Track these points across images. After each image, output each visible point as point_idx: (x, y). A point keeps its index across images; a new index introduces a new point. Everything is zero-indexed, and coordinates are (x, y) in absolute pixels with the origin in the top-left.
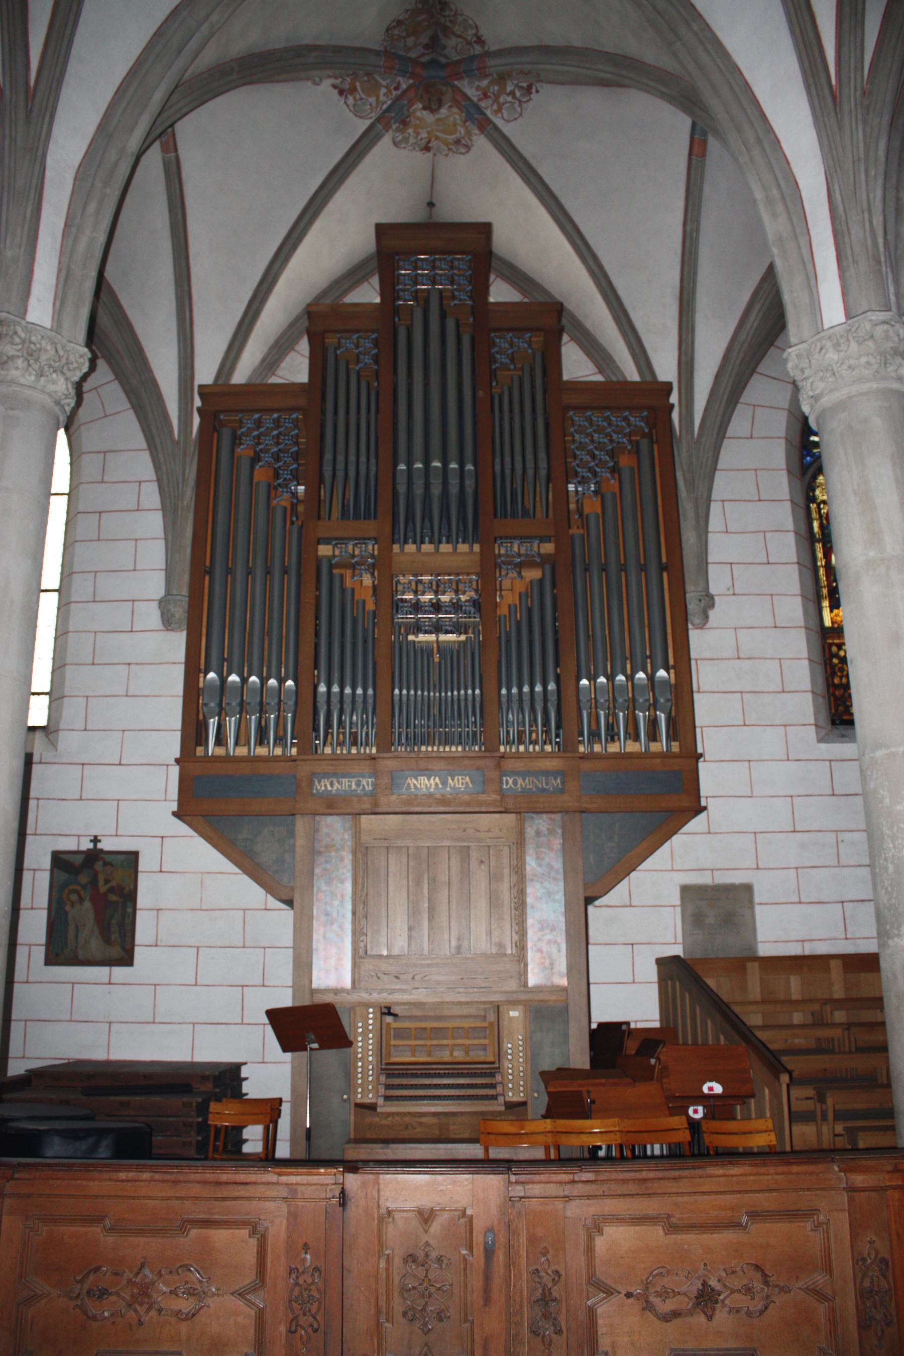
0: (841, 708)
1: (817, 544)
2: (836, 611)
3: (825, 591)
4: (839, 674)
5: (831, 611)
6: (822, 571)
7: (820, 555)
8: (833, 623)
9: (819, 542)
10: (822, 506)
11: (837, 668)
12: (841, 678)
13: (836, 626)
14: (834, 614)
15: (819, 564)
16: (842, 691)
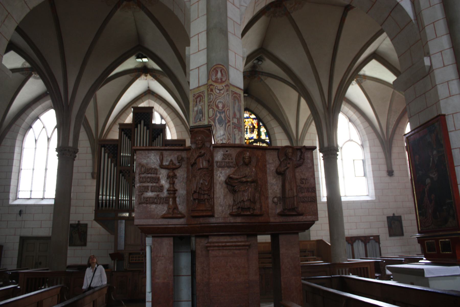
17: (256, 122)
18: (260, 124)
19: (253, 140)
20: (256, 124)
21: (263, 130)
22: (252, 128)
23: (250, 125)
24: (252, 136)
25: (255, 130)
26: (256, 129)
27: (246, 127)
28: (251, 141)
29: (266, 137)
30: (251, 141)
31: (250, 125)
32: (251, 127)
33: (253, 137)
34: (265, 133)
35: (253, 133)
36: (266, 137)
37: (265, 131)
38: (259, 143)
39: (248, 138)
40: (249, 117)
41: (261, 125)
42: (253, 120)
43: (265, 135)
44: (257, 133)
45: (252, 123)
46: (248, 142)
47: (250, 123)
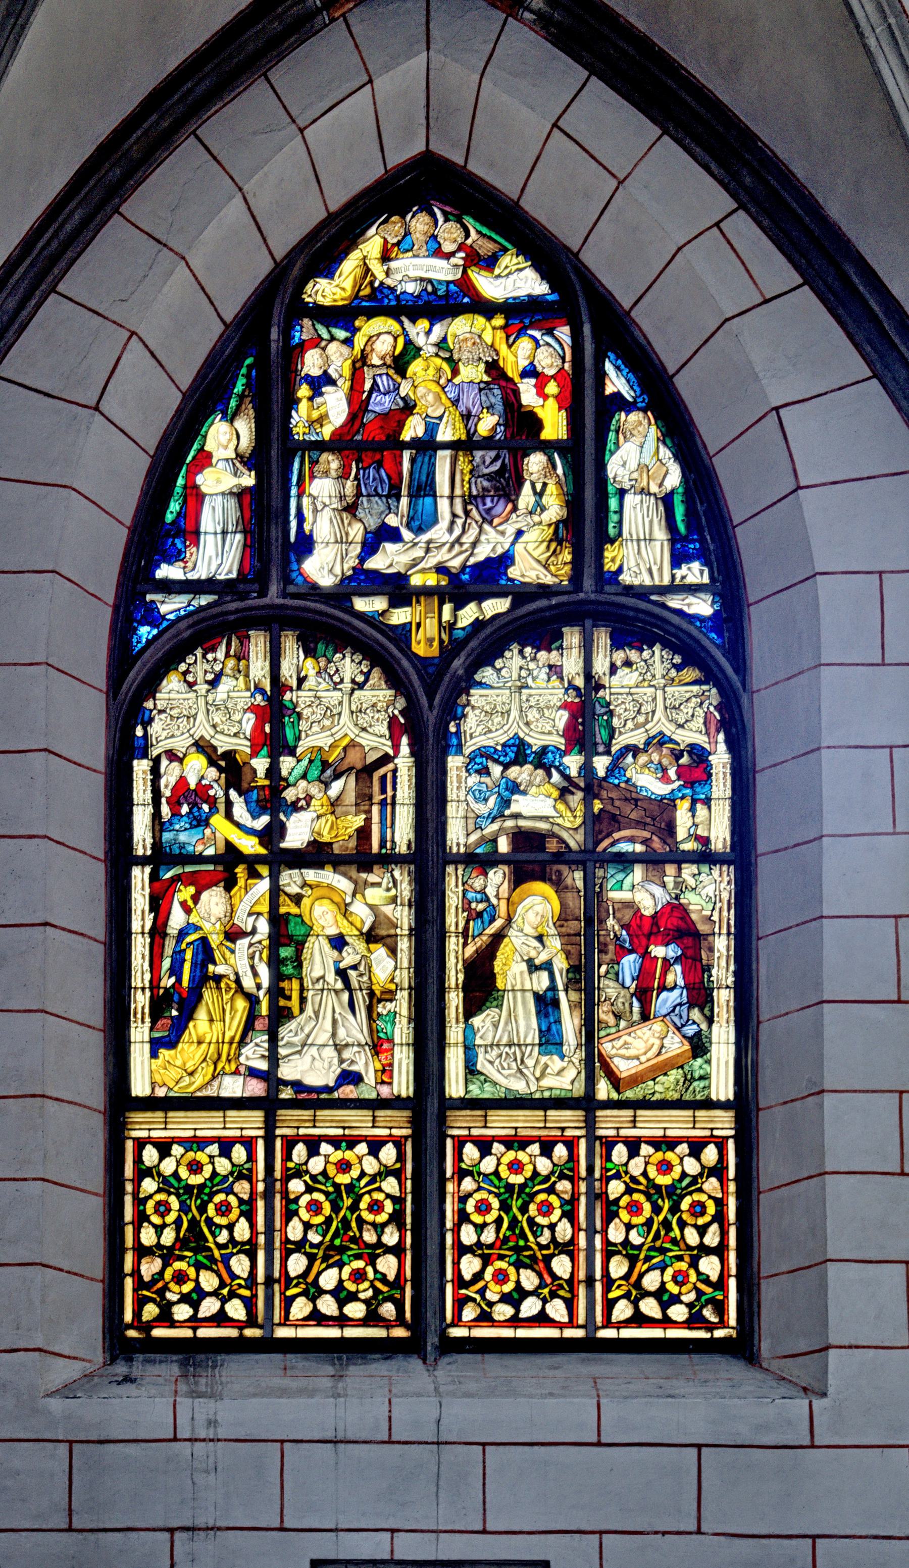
0: (150, 1311)
1: (136, 871)
2: (164, 1053)
3: (141, 1001)
4: (156, 1219)
5: (154, 1055)
6: (140, 947)
7: (140, 900)
8: (153, 1085)
9: (143, 861)
10: (164, 762)
11: (150, 1204)
12: (159, 1229)
13: (161, 1092)
14: (160, 1061)
15: (136, 926)
16: (158, 1263)
17: (547, 362)
18: (601, 377)
19: (496, 606)
20: (552, 388)
21: (643, 468)
22: (488, 443)
23: (470, 399)
24: (482, 553)
25: (535, 462)
26: (547, 447)
27: (413, 429)
28: (469, 614)
29: (677, 560)
30: (469, 614)
31: (470, 399)
32: (486, 424)
33: (506, 559)
34: (667, 500)
35: (503, 508)
36: (677, 560)
37: (674, 478)
38: (572, 637)
39: (432, 580)
40: (465, 284)
41: (618, 403)
42: (513, 332)
43: (661, 534)
44: (554, 509)
45: (494, 368)
46: (431, 628)
47: (473, 372)
